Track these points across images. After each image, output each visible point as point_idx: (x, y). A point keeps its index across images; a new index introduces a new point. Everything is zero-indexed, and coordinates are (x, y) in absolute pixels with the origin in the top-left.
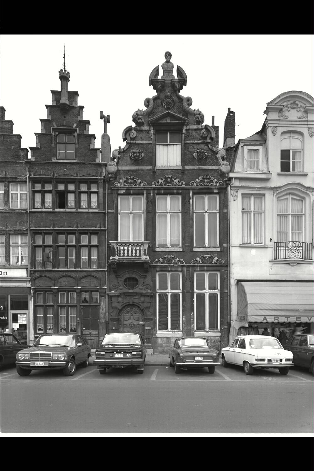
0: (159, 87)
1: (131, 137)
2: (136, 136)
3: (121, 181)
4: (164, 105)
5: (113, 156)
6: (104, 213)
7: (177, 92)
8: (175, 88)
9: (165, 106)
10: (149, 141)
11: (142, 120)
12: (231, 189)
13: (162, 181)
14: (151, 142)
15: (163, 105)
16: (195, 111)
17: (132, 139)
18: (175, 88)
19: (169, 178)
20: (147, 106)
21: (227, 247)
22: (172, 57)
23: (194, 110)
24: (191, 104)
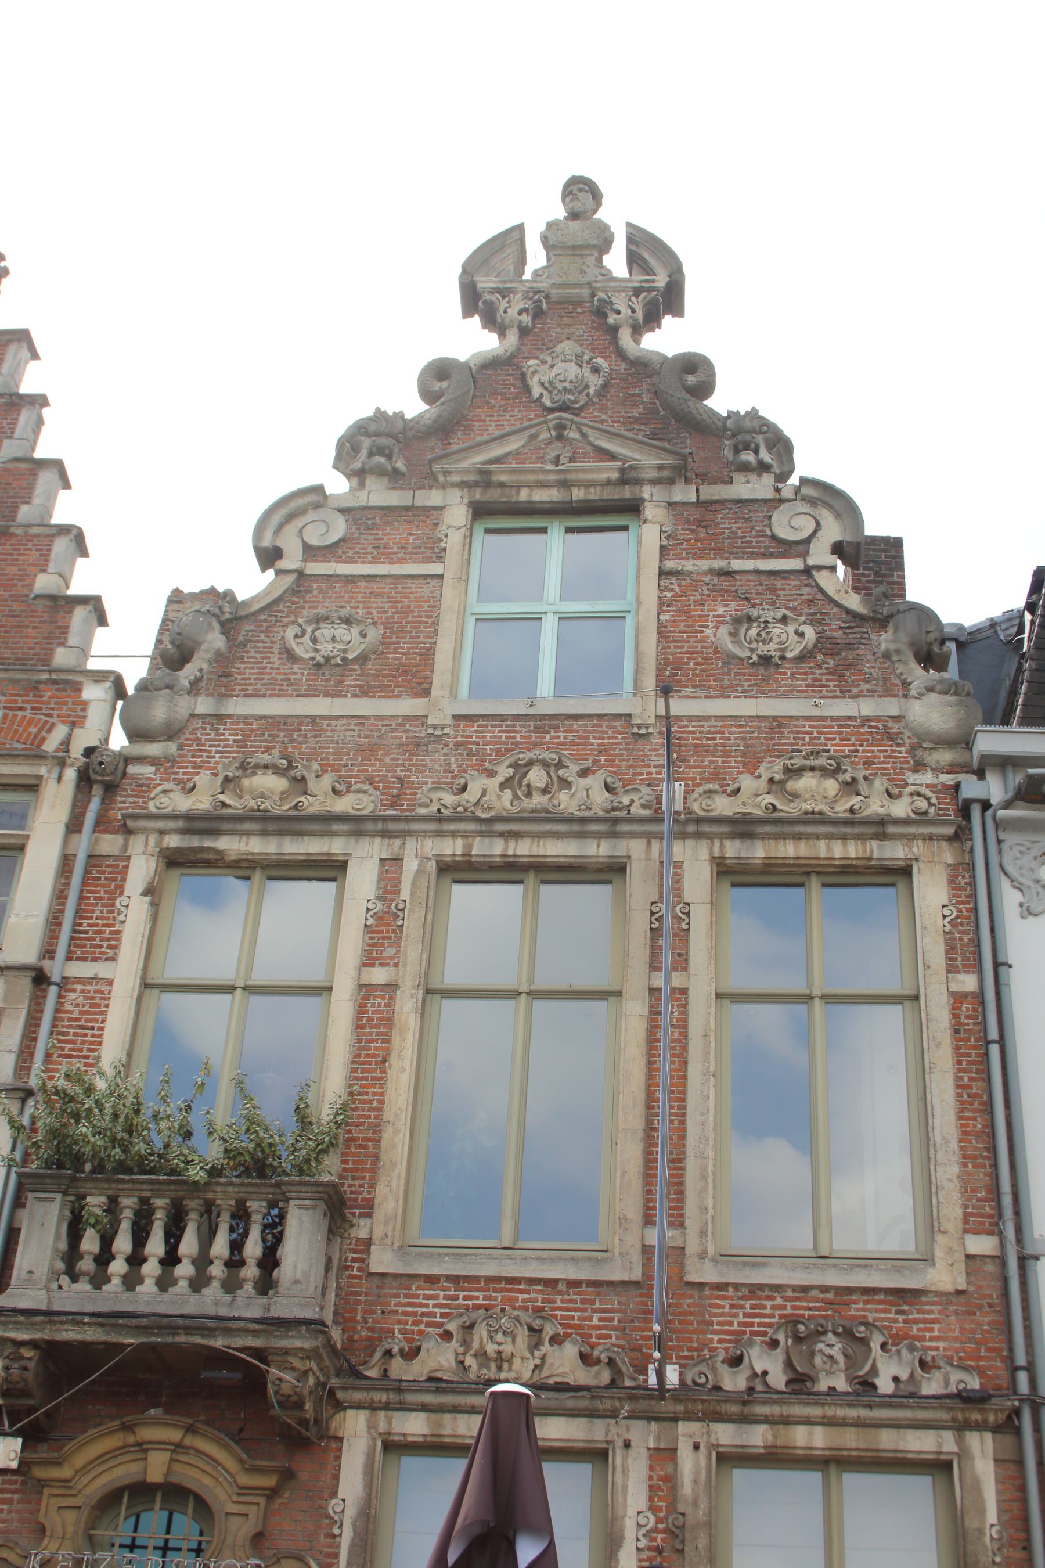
0: (513, 312)
1: (314, 541)
2: (343, 540)
3: (203, 779)
4: (536, 391)
5: (172, 642)
6: (40, 979)
7: (625, 337)
8: (611, 319)
9: (542, 395)
10: (428, 560)
11: (389, 457)
12: (999, 842)
13: (493, 783)
14: (435, 568)
15: (528, 389)
16: (729, 417)
17: (310, 552)
18: (611, 319)
19: (545, 764)
20: (427, 395)
21: (1001, 1260)
22: (604, 201)
23: (725, 414)
24: (706, 388)
